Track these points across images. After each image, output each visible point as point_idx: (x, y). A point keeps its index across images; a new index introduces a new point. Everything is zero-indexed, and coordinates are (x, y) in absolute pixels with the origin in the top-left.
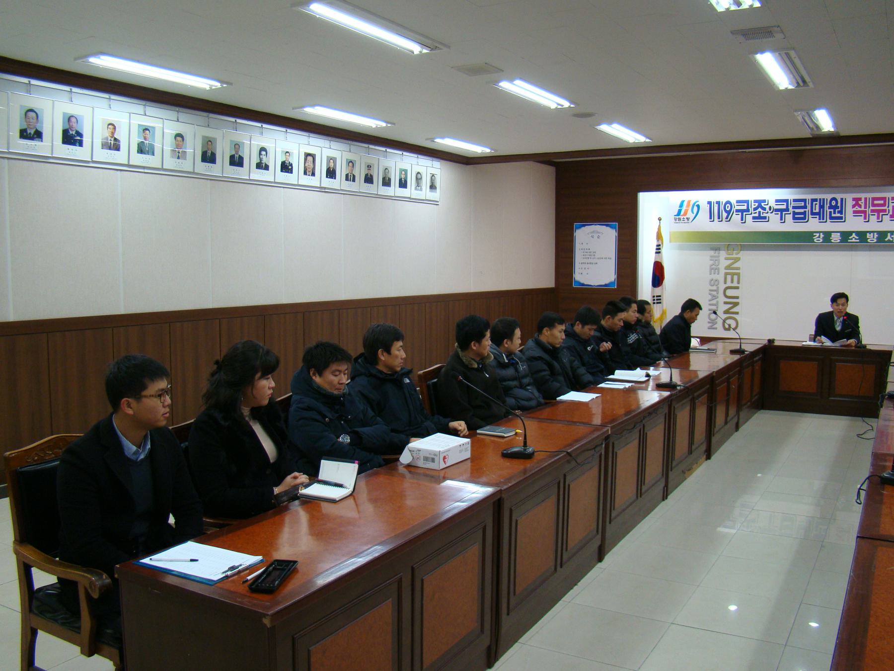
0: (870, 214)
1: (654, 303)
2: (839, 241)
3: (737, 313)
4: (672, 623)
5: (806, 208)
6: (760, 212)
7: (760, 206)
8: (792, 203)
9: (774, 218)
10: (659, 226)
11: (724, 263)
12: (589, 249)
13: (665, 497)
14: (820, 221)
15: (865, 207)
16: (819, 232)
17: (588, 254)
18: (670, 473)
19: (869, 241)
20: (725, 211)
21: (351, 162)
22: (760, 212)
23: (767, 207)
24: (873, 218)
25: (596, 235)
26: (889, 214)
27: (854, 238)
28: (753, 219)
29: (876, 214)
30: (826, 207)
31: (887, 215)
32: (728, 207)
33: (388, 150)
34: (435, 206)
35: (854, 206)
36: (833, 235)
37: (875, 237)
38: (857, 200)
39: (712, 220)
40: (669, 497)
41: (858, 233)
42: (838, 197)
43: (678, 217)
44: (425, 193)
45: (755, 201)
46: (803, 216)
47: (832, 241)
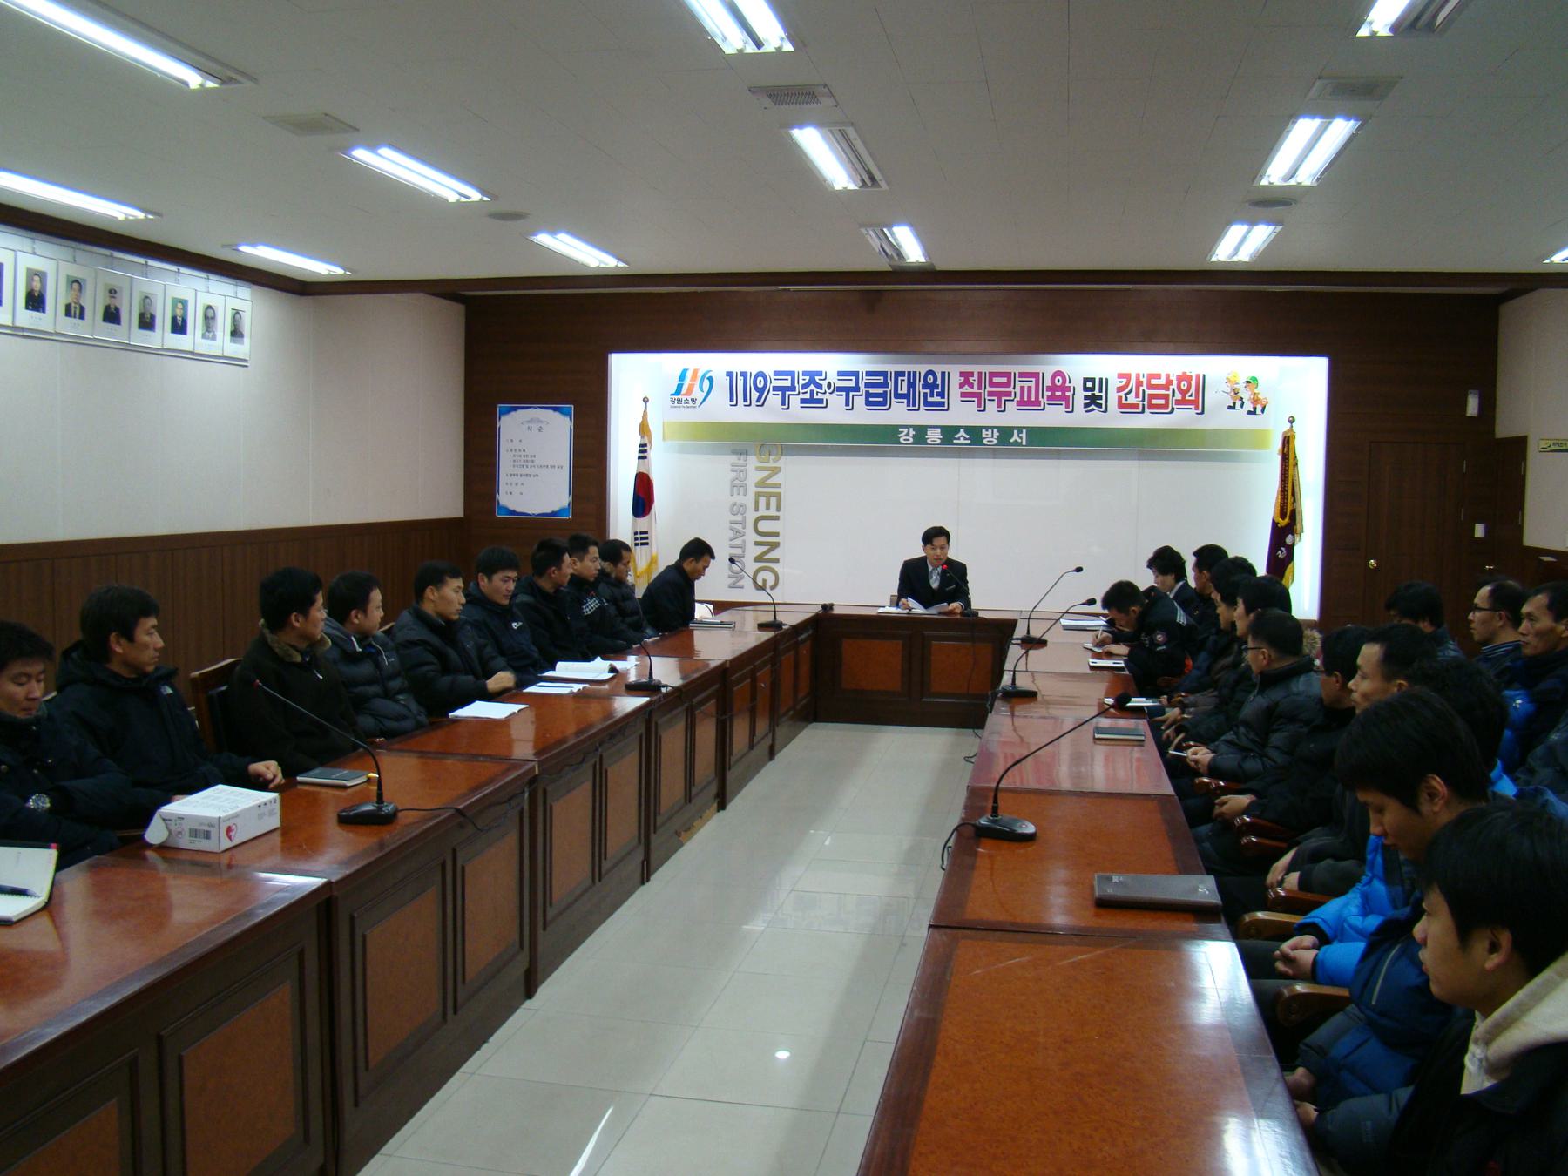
0: (987, 398)
1: (636, 545)
2: (939, 441)
3: (777, 561)
4: (651, 1095)
5: (888, 387)
6: (812, 392)
7: (812, 381)
9: (836, 401)
10: (645, 413)
11: (754, 477)
13: (645, 878)
15: (980, 388)
17: (523, 458)
18: (653, 837)
19: (985, 441)
20: (753, 389)
21: (77, 281)
22: (812, 392)
23: (825, 384)
24: (992, 406)
25: (535, 427)
29: (996, 398)
30: (919, 385)
31: (1013, 400)
33: (151, 263)
34: (241, 368)
35: (961, 386)
37: (995, 437)
38: (966, 375)
40: (652, 878)
41: (968, 429)
42: (938, 369)
43: (676, 397)
44: (223, 343)
45: (805, 373)
46: (882, 399)
47: (929, 441)
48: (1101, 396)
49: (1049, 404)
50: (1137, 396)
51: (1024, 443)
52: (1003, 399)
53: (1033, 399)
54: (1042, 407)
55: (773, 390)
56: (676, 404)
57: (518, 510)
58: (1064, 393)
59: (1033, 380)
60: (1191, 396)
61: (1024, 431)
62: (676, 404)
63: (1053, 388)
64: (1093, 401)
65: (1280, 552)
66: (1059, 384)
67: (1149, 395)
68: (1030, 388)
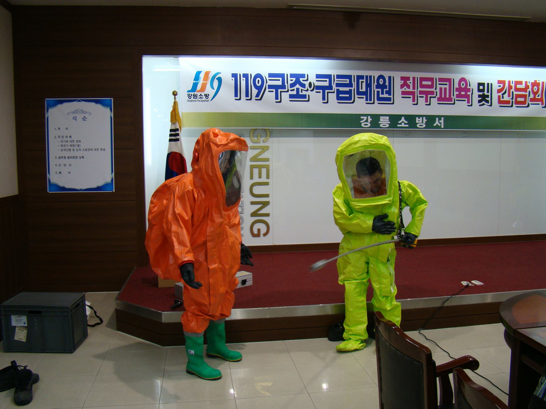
0: (419, 95)
2: (388, 126)
3: (268, 215)
5: (352, 87)
6: (298, 89)
7: (297, 82)
8: (336, 79)
9: (316, 96)
12: (70, 137)
15: (414, 88)
16: (367, 115)
17: (69, 144)
19: (418, 126)
22: (298, 89)
24: (422, 101)
25: (80, 116)
26: (437, 97)
28: (290, 98)
29: (424, 96)
30: (374, 85)
31: (435, 97)
32: (258, 81)
35: (402, 86)
37: (424, 122)
41: (407, 117)
42: (386, 74)
43: (192, 93)
45: (292, 76)
46: (348, 96)
47: (381, 125)
48: (488, 95)
49: (457, 100)
50: (509, 96)
51: (442, 127)
52: (429, 96)
53: (448, 96)
54: (453, 102)
55: (269, 88)
56: (192, 99)
57: (67, 186)
58: (466, 93)
59: (448, 83)
60: (538, 96)
61: (442, 118)
62: (192, 99)
63: (459, 89)
64: (483, 99)
66: (463, 87)
67: (516, 95)
68: (445, 89)
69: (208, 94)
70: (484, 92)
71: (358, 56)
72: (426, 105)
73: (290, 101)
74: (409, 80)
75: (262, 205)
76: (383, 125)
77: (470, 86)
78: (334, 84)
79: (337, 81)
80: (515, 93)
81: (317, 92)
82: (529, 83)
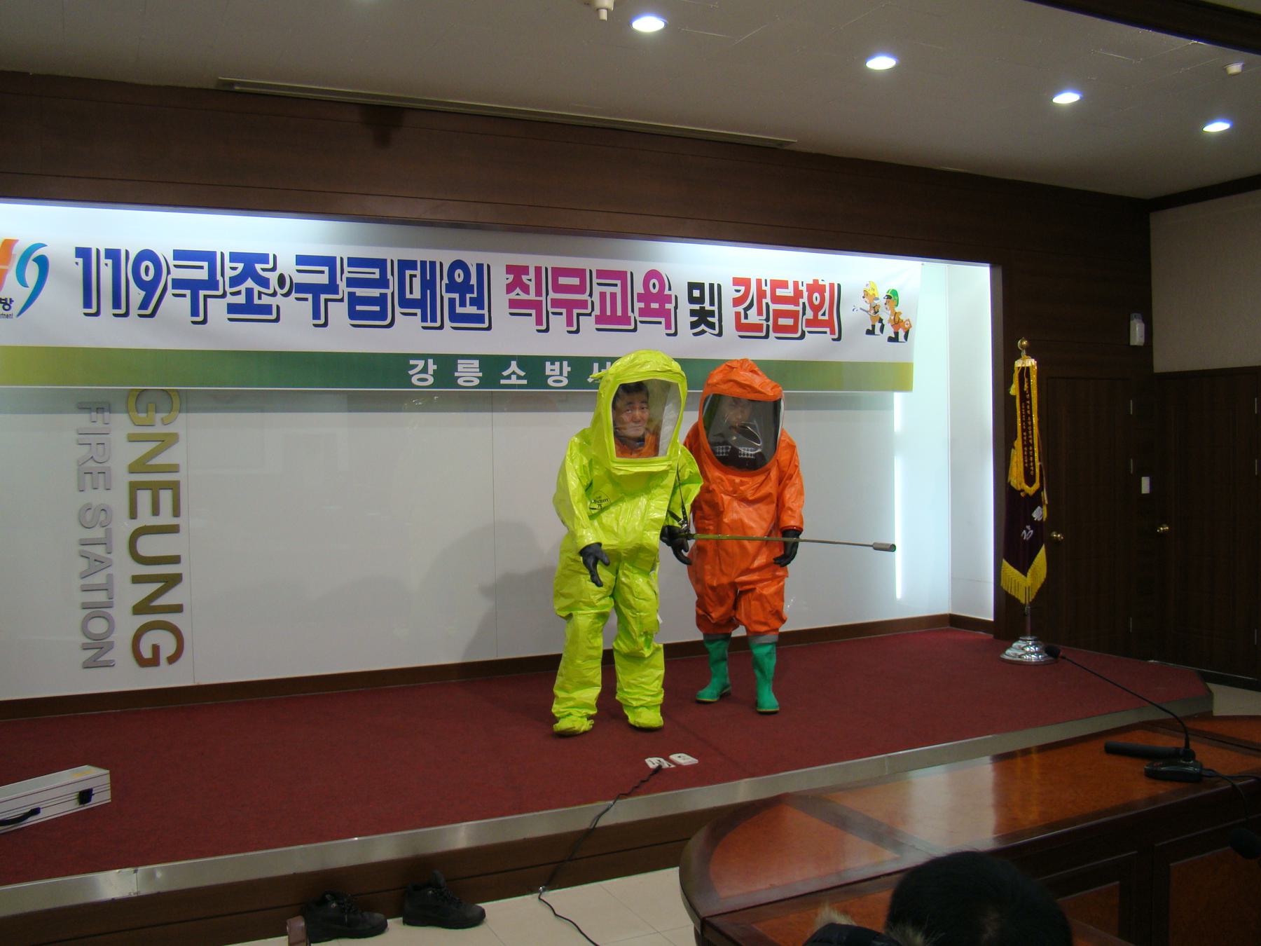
0: (551, 310)
2: (477, 382)
3: (178, 609)
5: (388, 288)
6: (249, 292)
7: (249, 272)
8: (346, 269)
9: (296, 310)
14: (425, 324)
15: (538, 293)
16: (424, 357)
19: (550, 381)
22: (249, 292)
23: (273, 278)
24: (558, 323)
26: (593, 314)
27: (514, 375)
28: (229, 312)
29: (564, 311)
30: (441, 284)
31: (590, 315)
32: (147, 269)
35: (510, 288)
36: (462, 365)
37: (565, 374)
38: (517, 272)
39: (94, 310)
41: (524, 361)
42: (472, 259)
45: (235, 257)
46: (377, 308)
47: (460, 382)
48: (713, 311)
49: (642, 322)
50: (760, 313)
52: (575, 311)
53: (619, 313)
54: (632, 327)
55: (174, 288)
58: (662, 306)
59: (619, 282)
60: (824, 314)
63: (646, 297)
64: (702, 319)
65: (1024, 531)
67: (775, 311)
68: (613, 296)
69: (10, 299)
70: (703, 303)
71: (397, 213)
72: (569, 332)
73: (230, 320)
74: (527, 273)
75: (163, 584)
76: (464, 381)
77: (670, 289)
78: (341, 280)
79: (349, 272)
80: (773, 307)
81: (298, 299)
82: (802, 285)
